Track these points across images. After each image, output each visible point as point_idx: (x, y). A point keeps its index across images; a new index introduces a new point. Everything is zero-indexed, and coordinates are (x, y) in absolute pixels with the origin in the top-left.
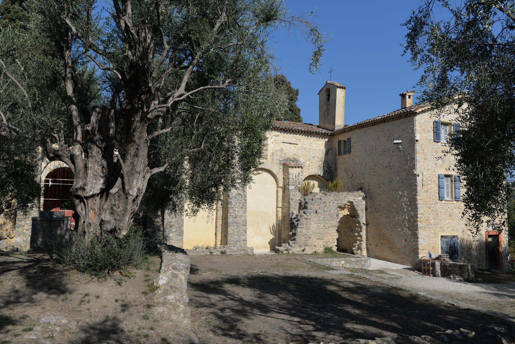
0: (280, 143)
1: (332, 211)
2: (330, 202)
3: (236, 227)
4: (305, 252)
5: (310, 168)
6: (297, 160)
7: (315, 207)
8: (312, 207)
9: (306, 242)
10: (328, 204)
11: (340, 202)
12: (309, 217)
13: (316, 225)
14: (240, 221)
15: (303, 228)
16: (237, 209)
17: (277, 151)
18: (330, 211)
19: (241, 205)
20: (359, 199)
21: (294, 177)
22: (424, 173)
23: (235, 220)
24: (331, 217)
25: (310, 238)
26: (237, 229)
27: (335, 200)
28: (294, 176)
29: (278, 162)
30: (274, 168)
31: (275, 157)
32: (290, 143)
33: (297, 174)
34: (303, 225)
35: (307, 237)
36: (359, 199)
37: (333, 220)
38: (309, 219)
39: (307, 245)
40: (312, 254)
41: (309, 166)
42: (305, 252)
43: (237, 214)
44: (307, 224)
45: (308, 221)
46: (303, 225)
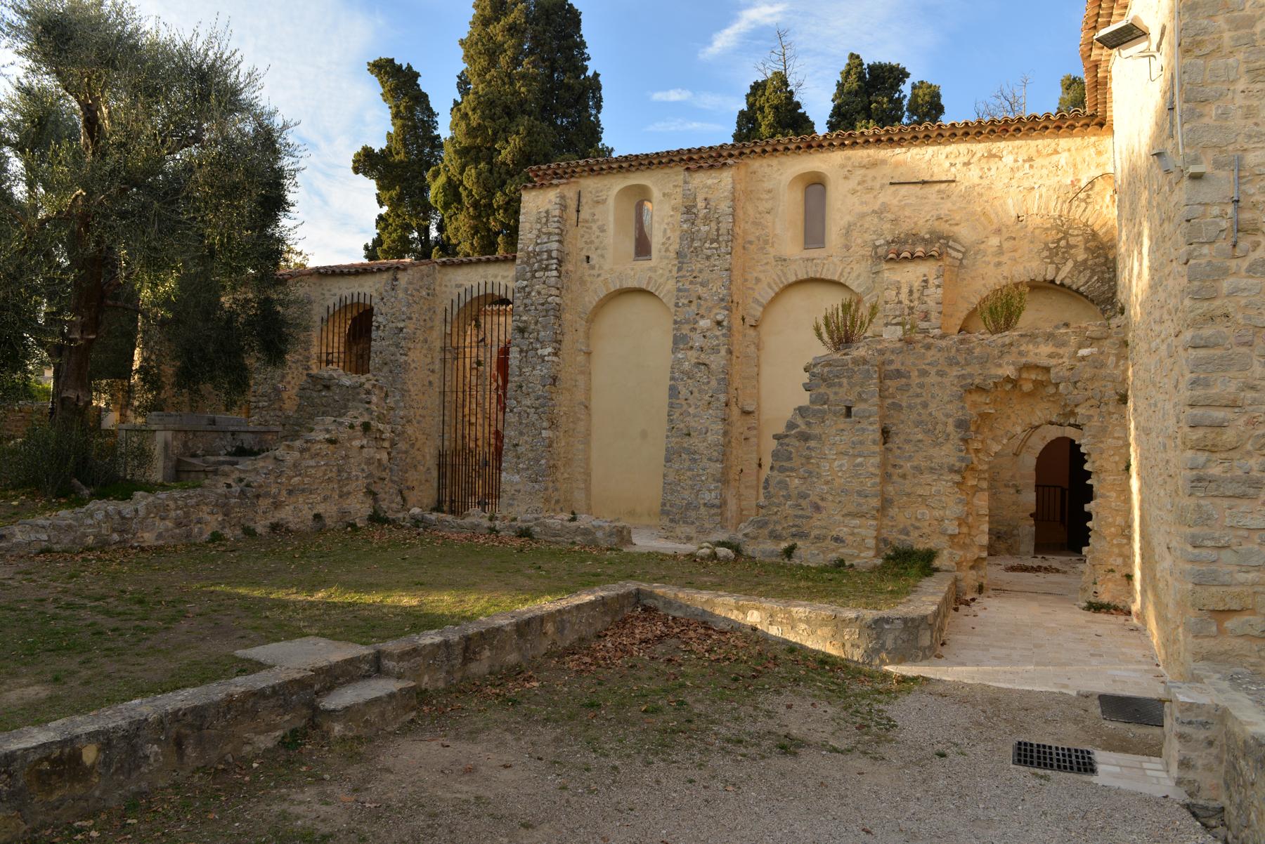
0: (882, 187)
1: (932, 407)
2: (924, 373)
3: (687, 464)
4: (796, 561)
5: (1004, 259)
6: (947, 238)
7: (842, 391)
8: (830, 392)
9: (798, 522)
10: (915, 379)
11: (974, 369)
12: (816, 431)
13: (844, 461)
14: (701, 447)
15: (792, 470)
16: (691, 410)
17: (863, 216)
18: (925, 405)
19: (707, 398)
20: (1084, 352)
21: (904, 296)
22: (1251, 159)
23: (686, 442)
24: (927, 432)
25: (817, 508)
26: (690, 469)
27: (952, 362)
28: (905, 290)
29: (868, 251)
30: (854, 275)
31: (857, 239)
32: (924, 182)
33: (917, 285)
34: (790, 459)
35: (804, 503)
36: (1084, 352)
37: (936, 444)
38: (818, 438)
39: (803, 535)
40: (823, 570)
41: (1000, 250)
42: (796, 561)
43: (693, 424)
44: (809, 458)
45: (812, 444)
46: (790, 459)
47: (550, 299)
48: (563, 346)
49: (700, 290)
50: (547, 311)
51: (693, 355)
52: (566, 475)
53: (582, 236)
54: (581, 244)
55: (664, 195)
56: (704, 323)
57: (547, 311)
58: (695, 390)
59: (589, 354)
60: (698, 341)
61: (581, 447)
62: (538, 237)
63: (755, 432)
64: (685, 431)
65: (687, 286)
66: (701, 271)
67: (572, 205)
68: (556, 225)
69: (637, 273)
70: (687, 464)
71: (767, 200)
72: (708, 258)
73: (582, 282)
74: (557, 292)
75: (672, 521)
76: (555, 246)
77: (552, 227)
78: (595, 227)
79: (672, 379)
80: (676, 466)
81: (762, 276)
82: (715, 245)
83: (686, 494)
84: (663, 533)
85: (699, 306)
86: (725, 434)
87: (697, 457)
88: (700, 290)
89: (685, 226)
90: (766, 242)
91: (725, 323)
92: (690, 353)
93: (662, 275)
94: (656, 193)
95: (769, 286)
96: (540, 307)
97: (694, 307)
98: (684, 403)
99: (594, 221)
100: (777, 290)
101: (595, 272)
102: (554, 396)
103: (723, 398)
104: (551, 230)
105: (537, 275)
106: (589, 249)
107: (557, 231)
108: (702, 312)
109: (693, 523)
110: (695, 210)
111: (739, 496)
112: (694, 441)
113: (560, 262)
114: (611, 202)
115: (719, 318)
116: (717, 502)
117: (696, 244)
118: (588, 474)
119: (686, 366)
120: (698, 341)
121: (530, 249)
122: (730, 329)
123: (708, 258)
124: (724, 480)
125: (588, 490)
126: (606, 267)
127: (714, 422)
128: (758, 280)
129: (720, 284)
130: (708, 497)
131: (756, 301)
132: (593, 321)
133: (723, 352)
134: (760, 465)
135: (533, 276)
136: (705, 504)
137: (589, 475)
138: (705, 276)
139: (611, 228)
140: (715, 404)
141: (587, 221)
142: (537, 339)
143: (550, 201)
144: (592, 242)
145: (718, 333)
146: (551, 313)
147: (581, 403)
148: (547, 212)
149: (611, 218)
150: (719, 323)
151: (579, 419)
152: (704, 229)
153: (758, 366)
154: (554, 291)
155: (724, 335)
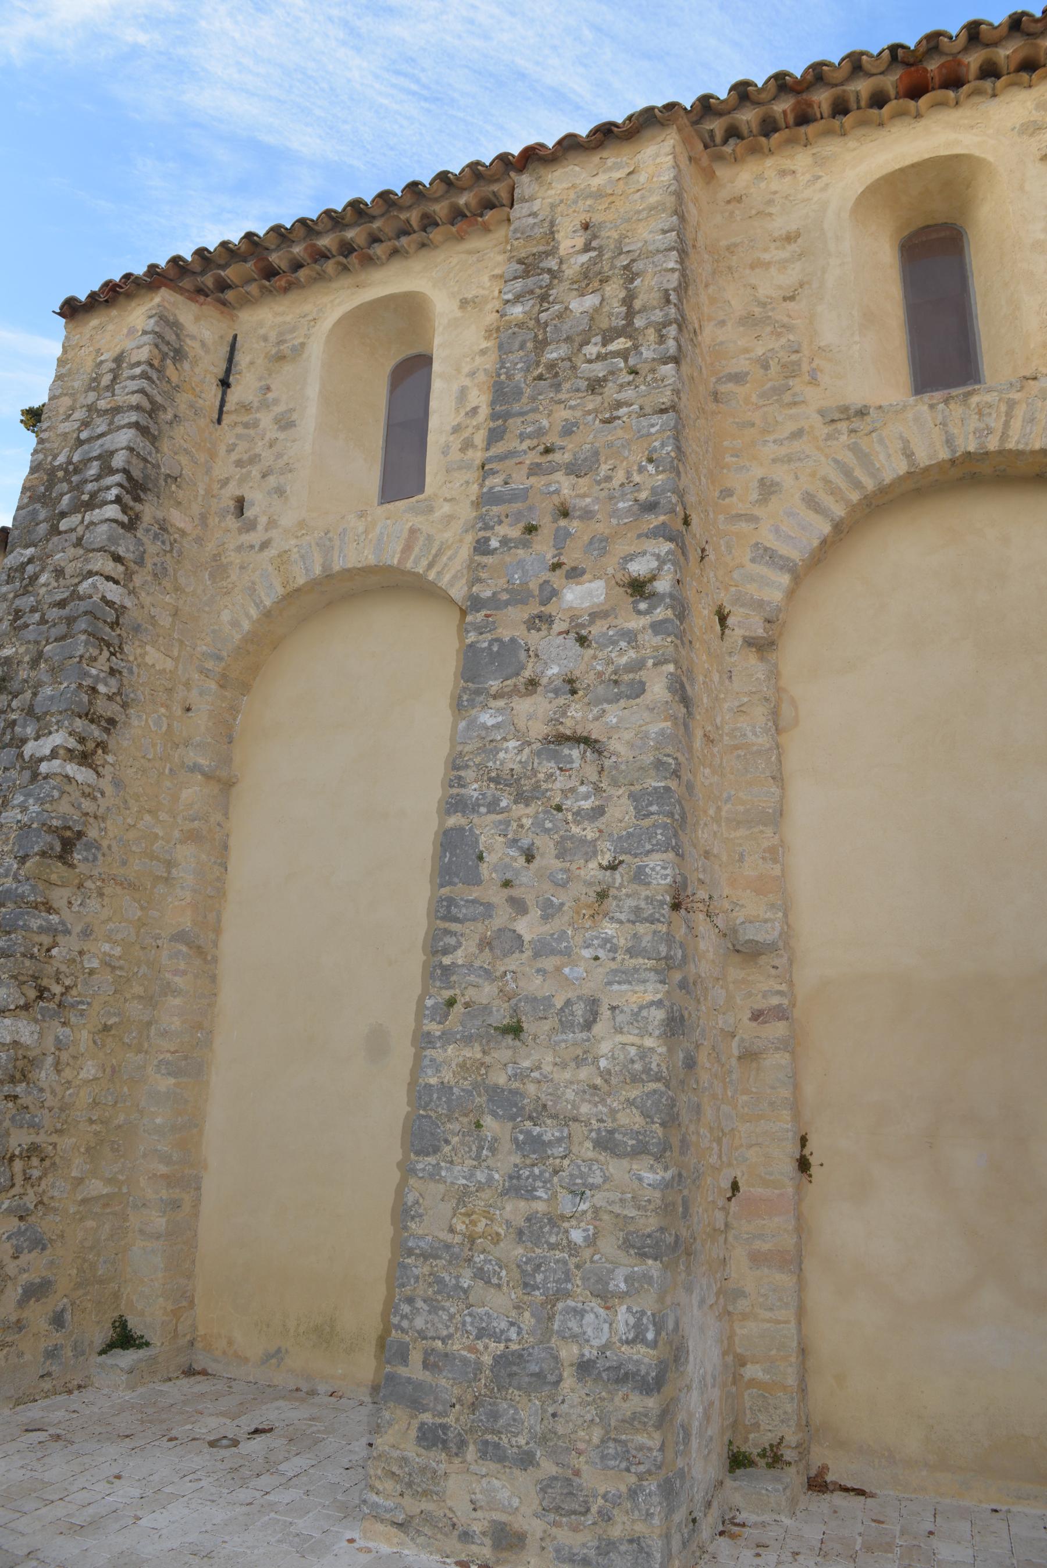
3: (507, 1160)
14: (568, 1085)
16: (527, 927)
19: (592, 870)
23: (502, 1065)
26: (517, 1187)
43: (535, 985)
47: (84, 587)
48: (123, 741)
49: (565, 486)
50: (70, 621)
51: (534, 713)
52: (96, 1187)
53: (231, 449)
54: (223, 468)
55: (464, 303)
56: (579, 596)
57: (70, 621)
58: (546, 845)
59: (228, 785)
60: (557, 658)
61: (165, 1083)
62: (86, 424)
63: (778, 1029)
64: (501, 1016)
65: (520, 481)
66: (568, 430)
67: (208, 366)
68: (133, 385)
69: (377, 535)
70: (507, 1160)
71: (783, 265)
72: (595, 386)
73: (218, 569)
74: (116, 570)
75: (431, 1437)
76: (124, 437)
77: (127, 393)
78: (266, 419)
79: (455, 804)
80: (457, 1175)
81: (780, 474)
82: (620, 344)
83: (497, 1303)
84: (386, 1496)
85: (561, 539)
86: (675, 1025)
87: (549, 1131)
88: (565, 486)
89: (517, 311)
90: (791, 370)
91: (662, 586)
92: (523, 706)
93: (450, 518)
94: (443, 305)
95: (811, 501)
96: (54, 614)
97: (543, 548)
98: (497, 896)
99: (265, 405)
100: (839, 511)
101: (254, 538)
102: (59, 897)
103: (660, 868)
104: (120, 399)
105: (63, 525)
106: (243, 480)
107: (135, 399)
108: (572, 557)
109: (526, 1460)
110: (552, 263)
111: (727, 1301)
112: (542, 1063)
113: (136, 488)
114: (316, 350)
115: (639, 568)
116: (643, 1356)
117: (552, 354)
118: (185, 1180)
119: (510, 756)
120: (557, 658)
121: (61, 459)
122: (682, 610)
123: (595, 386)
124: (669, 1245)
125: (181, 1241)
126: (287, 520)
127: (627, 976)
128: (768, 489)
129: (637, 456)
130: (601, 1328)
131: (768, 555)
132: (245, 688)
133: (658, 689)
134: (804, 1165)
135: (55, 531)
136: (584, 1368)
137: (195, 1185)
138: (591, 436)
139: (310, 416)
140: (628, 897)
141: (246, 408)
142: (30, 711)
143: (131, 331)
144: (255, 459)
145: (635, 623)
146: (82, 624)
147: (180, 937)
148: (119, 360)
149: (313, 390)
150: (638, 587)
151: (168, 989)
152: (581, 305)
153: (778, 778)
154: (102, 563)
155: (657, 627)
